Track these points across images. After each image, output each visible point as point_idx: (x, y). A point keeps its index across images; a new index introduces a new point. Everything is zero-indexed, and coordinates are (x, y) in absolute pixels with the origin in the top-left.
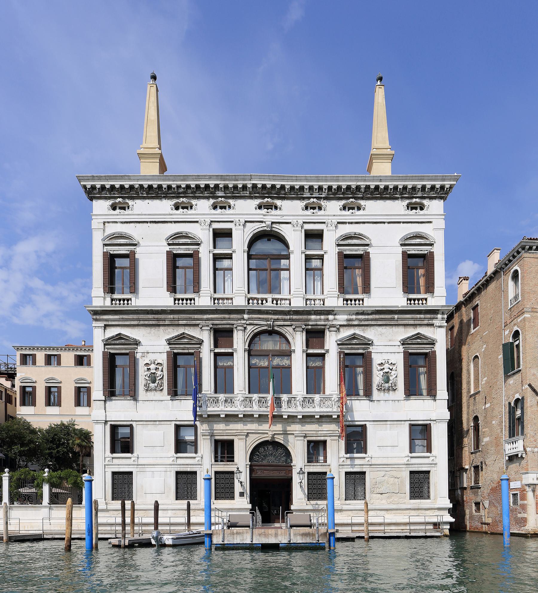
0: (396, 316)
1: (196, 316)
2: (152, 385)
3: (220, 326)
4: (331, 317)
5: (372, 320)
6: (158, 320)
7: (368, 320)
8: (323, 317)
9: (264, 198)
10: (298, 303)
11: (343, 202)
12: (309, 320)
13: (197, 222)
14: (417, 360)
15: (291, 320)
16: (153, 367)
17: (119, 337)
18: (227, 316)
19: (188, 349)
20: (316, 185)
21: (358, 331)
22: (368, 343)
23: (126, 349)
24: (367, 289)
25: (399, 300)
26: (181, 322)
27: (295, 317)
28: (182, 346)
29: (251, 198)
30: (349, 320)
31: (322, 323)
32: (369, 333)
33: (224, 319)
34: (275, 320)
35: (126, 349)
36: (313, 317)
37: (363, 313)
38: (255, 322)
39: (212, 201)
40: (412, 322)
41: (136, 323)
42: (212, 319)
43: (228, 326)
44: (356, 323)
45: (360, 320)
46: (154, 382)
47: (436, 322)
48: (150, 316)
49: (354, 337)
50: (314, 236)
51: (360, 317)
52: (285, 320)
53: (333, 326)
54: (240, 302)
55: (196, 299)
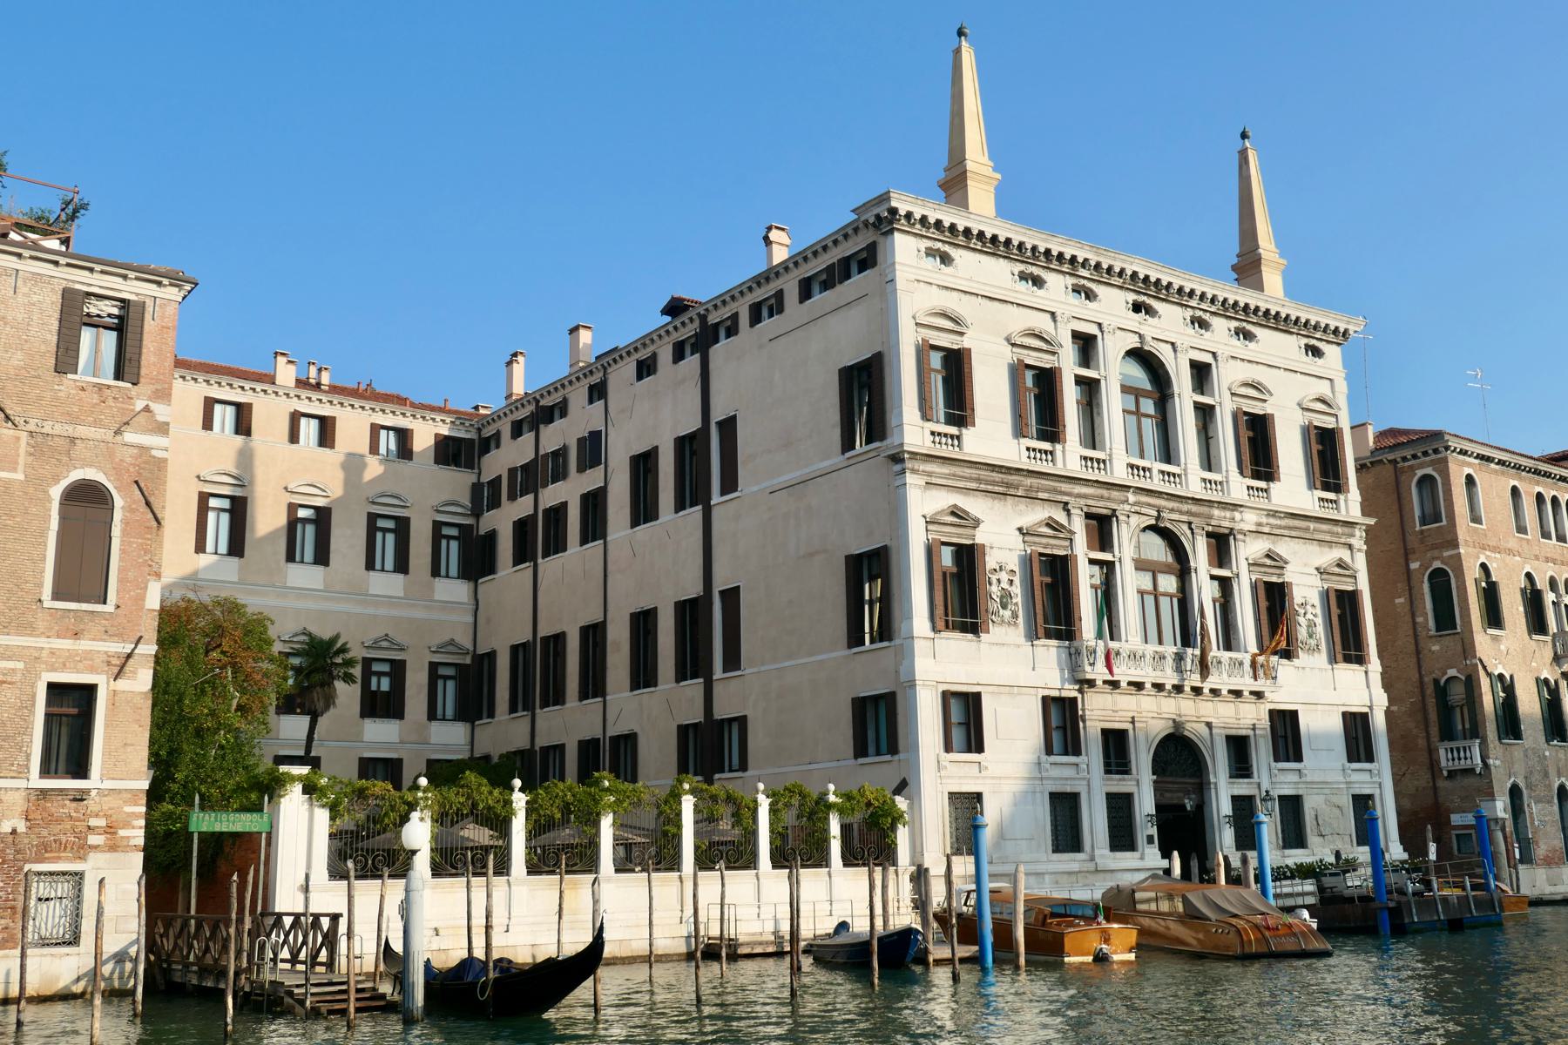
0: (1312, 525)
1: (1065, 487)
2: (1007, 614)
3: (1094, 510)
4: (1237, 515)
5: (1285, 528)
6: (1008, 485)
7: (1280, 527)
8: (1228, 514)
9: (1139, 293)
10: (1194, 487)
12: (1211, 517)
13: (1053, 314)
14: (1344, 606)
16: (1004, 576)
17: (955, 512)
18: (1105, 493)
19: (1053, 546)
23: (959, 535)
26: (1041, 495)
27: (1194, 508)
28: (1044, 540)
29: (1121, 288)
30: (1260, 524)
31: (1227, 524)
32: (1283, 548)
33: (1102, 498)
34: (1172, 510)
35: (959, 535)
36: (1216, 512)
37: (1273, 514)
38: (1144, 510)
40: (1328, 538)
41: (973, 485)
42: (1085, 496)
43: (1105, 512)
44: (1266, 530)
45: (1272, 526)
46: (1004, 607)
48: (997, 476)
50: (1201, 373)
52: (1181, 513)
55: (1059, 454)
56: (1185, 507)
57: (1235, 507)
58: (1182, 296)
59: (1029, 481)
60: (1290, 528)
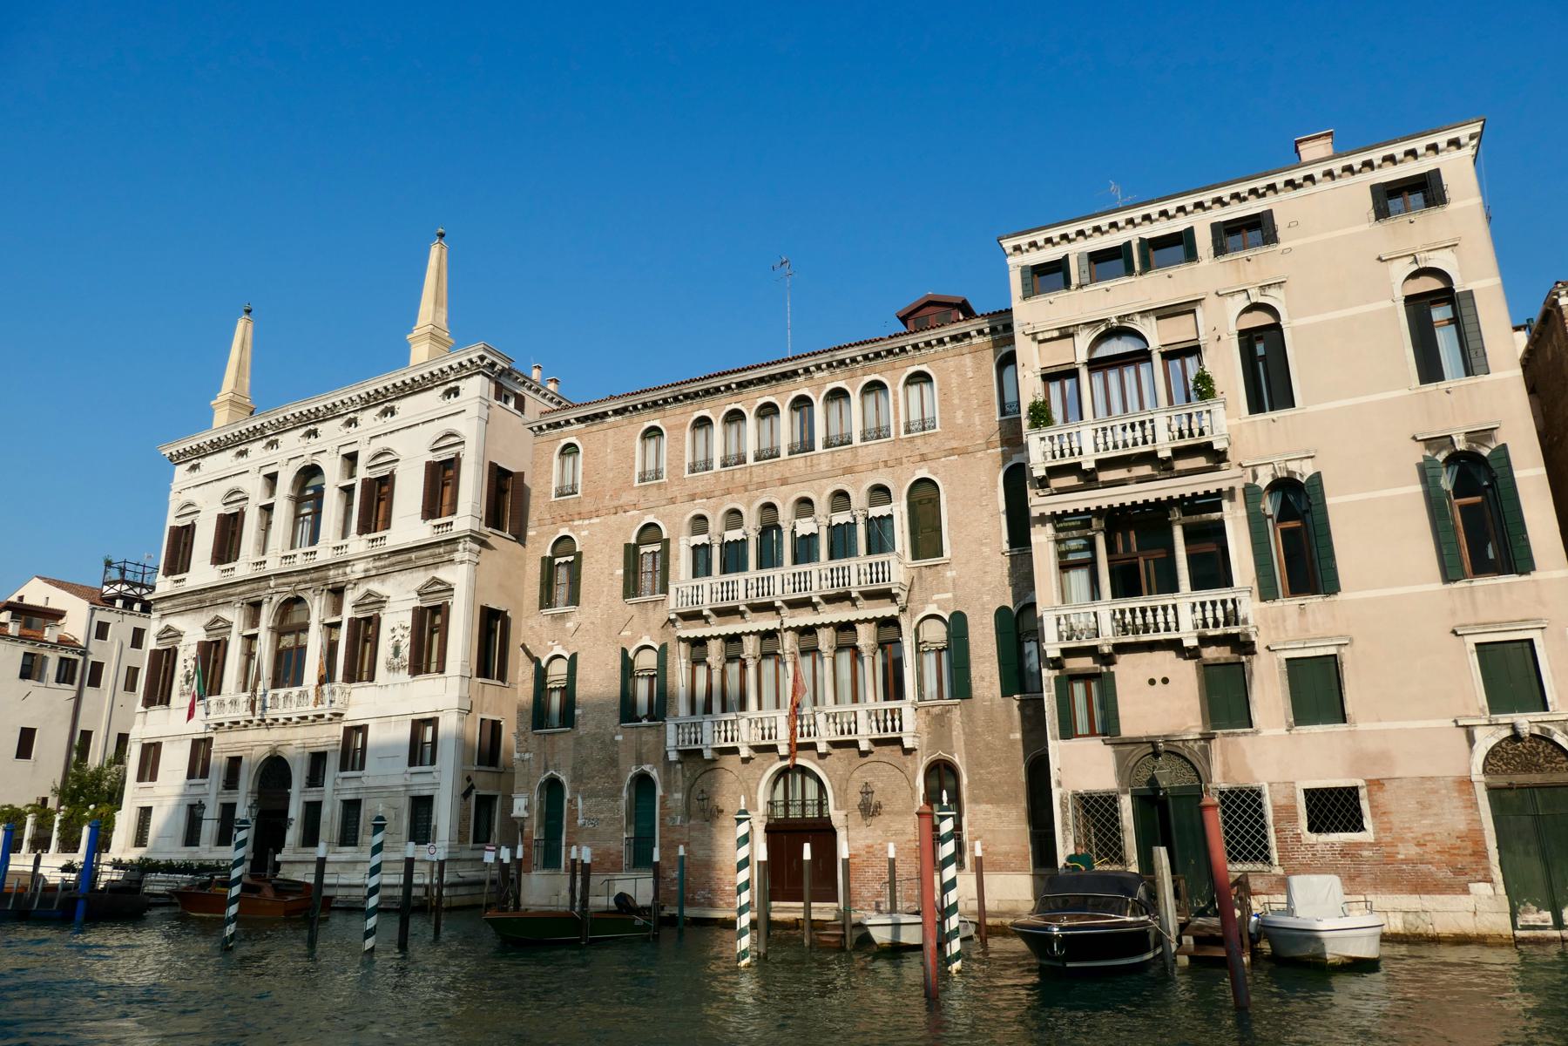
0: (413, 556)
1: (231, 591)
4: (348, 570)
5: (393, 565)
11: (381, 408)
15: (312, 581)
20: (345, 398)
21: (375, 586)
22: (381, 602)
24: (387, 526)
25: (424, 532)
27: (315, 575)
36: (332, 573)
39: (265, 441)
40: (431, 561)
44: (373, 572)
47: (457, 556)
49: (369, 594)
51: (378, 564)
53: (349, 582)
54: (273, 565)
56: (308, 577)
57: (345, 563)
58: (331, 413)
59: (211, 595)
60: (393, 565)
